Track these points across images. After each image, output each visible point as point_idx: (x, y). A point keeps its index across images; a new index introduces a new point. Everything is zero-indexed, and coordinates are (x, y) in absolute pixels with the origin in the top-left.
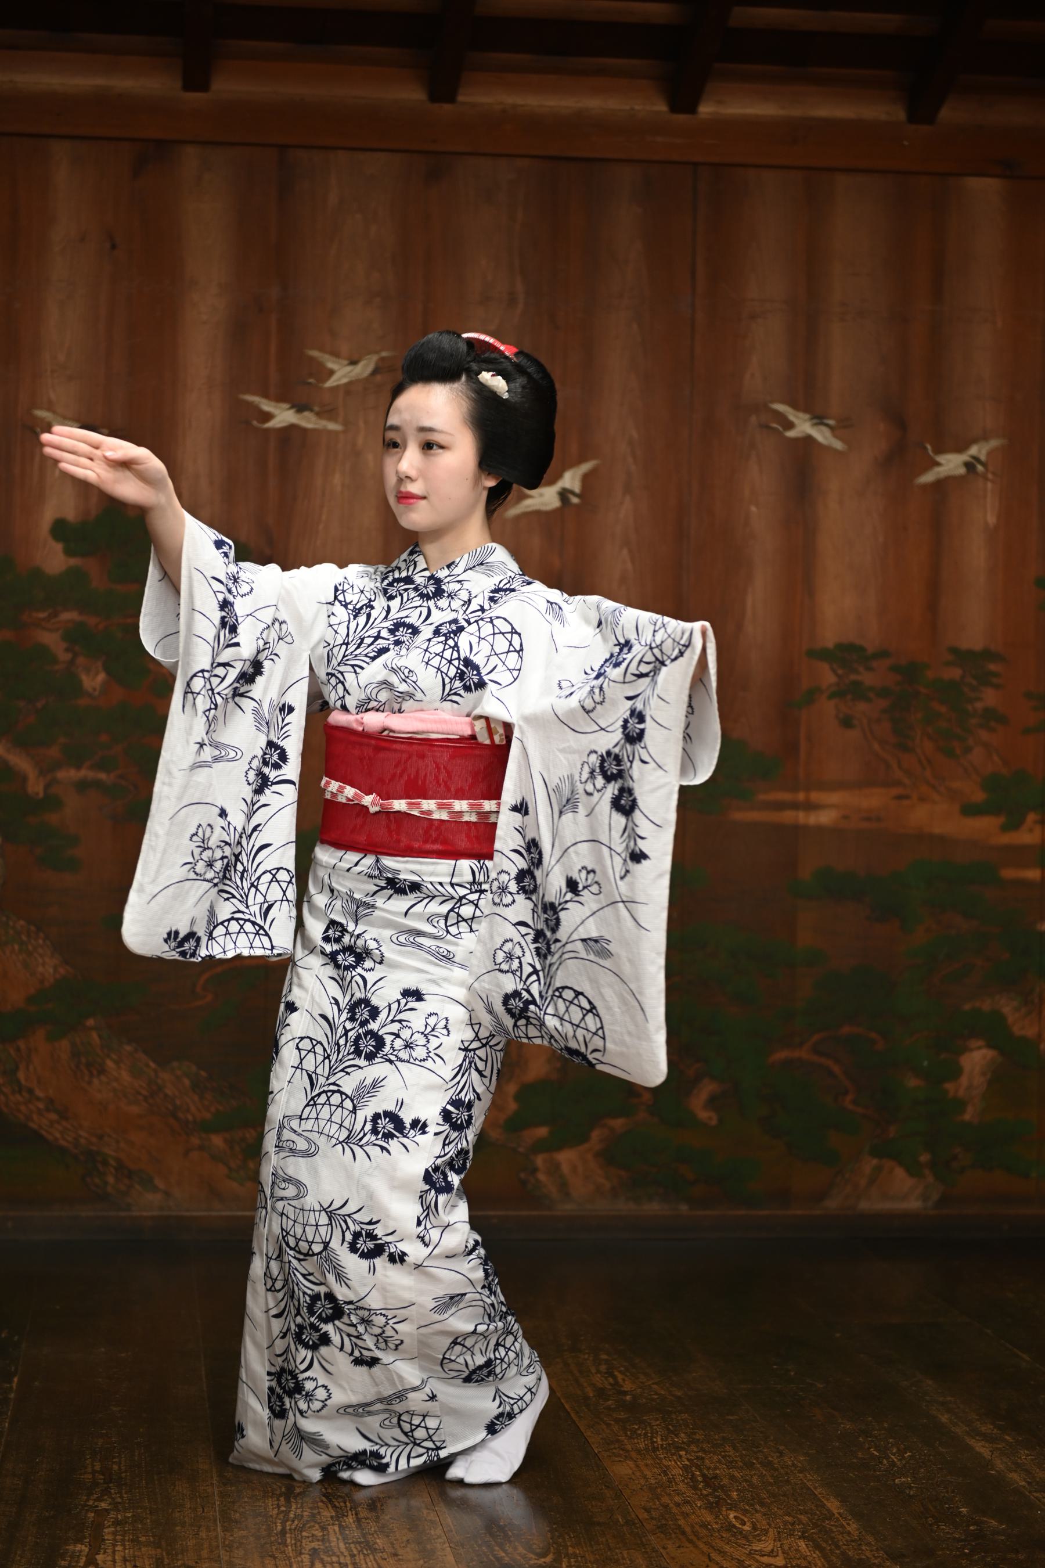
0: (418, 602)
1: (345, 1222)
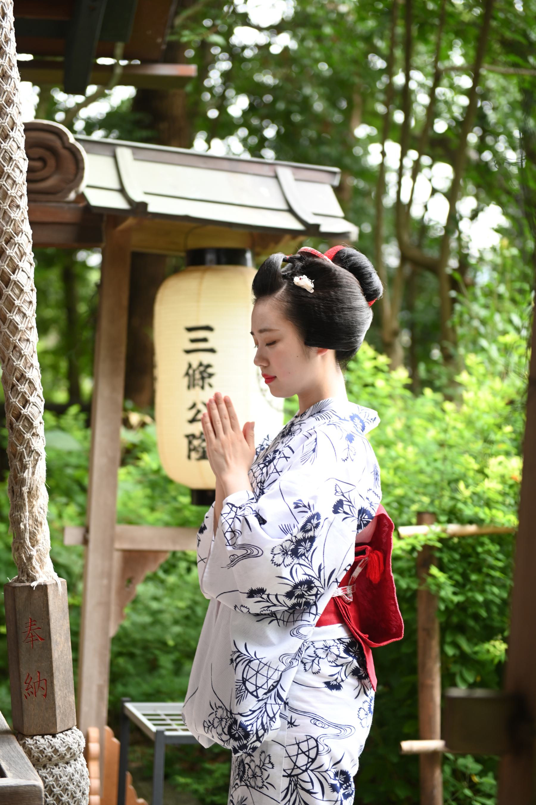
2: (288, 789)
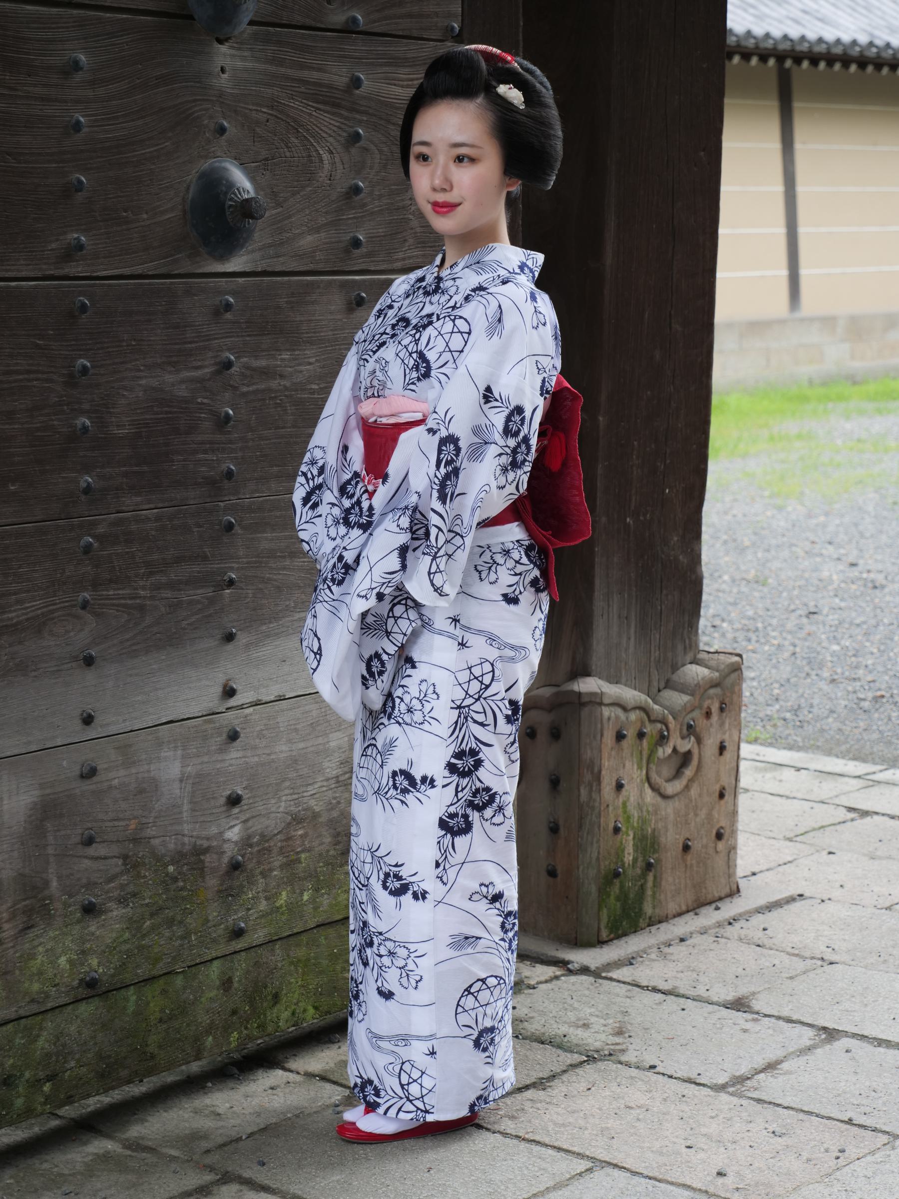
2: (456, 723)
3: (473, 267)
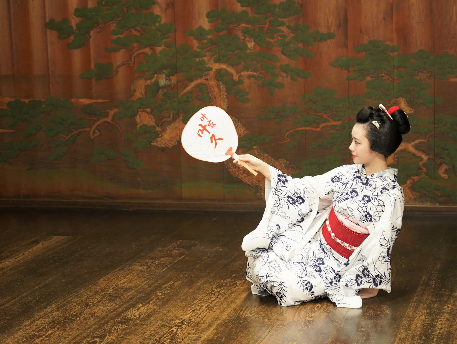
0: (361, 184)
1: (281, 289)
3: (380, 178)
